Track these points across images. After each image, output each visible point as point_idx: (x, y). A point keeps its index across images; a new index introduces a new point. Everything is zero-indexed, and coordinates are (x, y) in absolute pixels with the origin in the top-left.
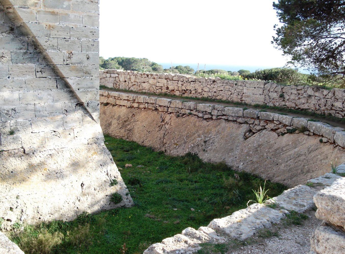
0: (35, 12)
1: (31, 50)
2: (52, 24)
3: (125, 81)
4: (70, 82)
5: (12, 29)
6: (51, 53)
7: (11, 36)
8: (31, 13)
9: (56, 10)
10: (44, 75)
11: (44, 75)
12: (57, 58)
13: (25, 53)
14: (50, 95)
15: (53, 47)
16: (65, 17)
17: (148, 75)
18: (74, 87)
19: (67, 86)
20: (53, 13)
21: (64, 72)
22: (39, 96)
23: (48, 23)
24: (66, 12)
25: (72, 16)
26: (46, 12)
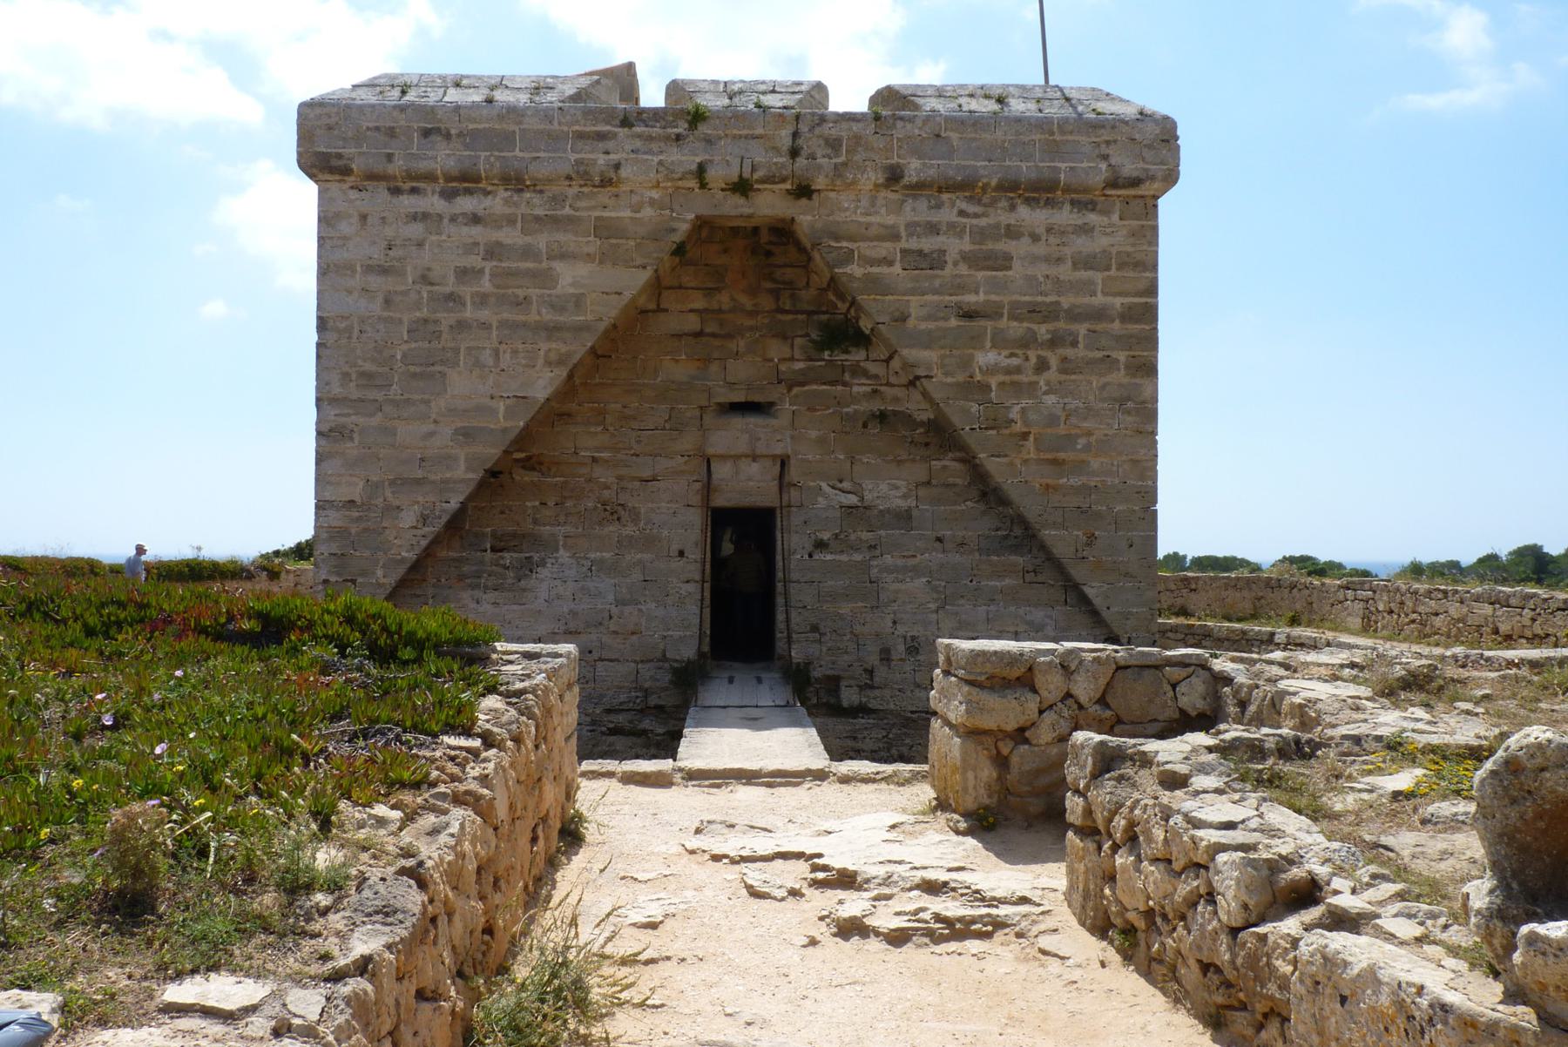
0: (1018, 462)
1: (1018, 531)
2: (1049, 481)
3: (1391, 612)
4: (1089, 591)
5: (984, 495)
6: (1048, 534)
7: (982, 507)
8: (1012, 464)
9: (1062, 455)
10: (1040, 578)
11: (1040, 578)
12: (1061, 541)
13: (1006, 537)
14: (1050, 617)
15: (1054, 525)
16: (1080, 467)
17: (1445, 592)
18: (1098, 602)
19: (1084, 600)
20: (1055, 462)
21: (1078, 573)
22: (1028, 618)
23: (1044, 481)
24: (1083, 456)
25: (1095, 464)
26: (1040, 461)
